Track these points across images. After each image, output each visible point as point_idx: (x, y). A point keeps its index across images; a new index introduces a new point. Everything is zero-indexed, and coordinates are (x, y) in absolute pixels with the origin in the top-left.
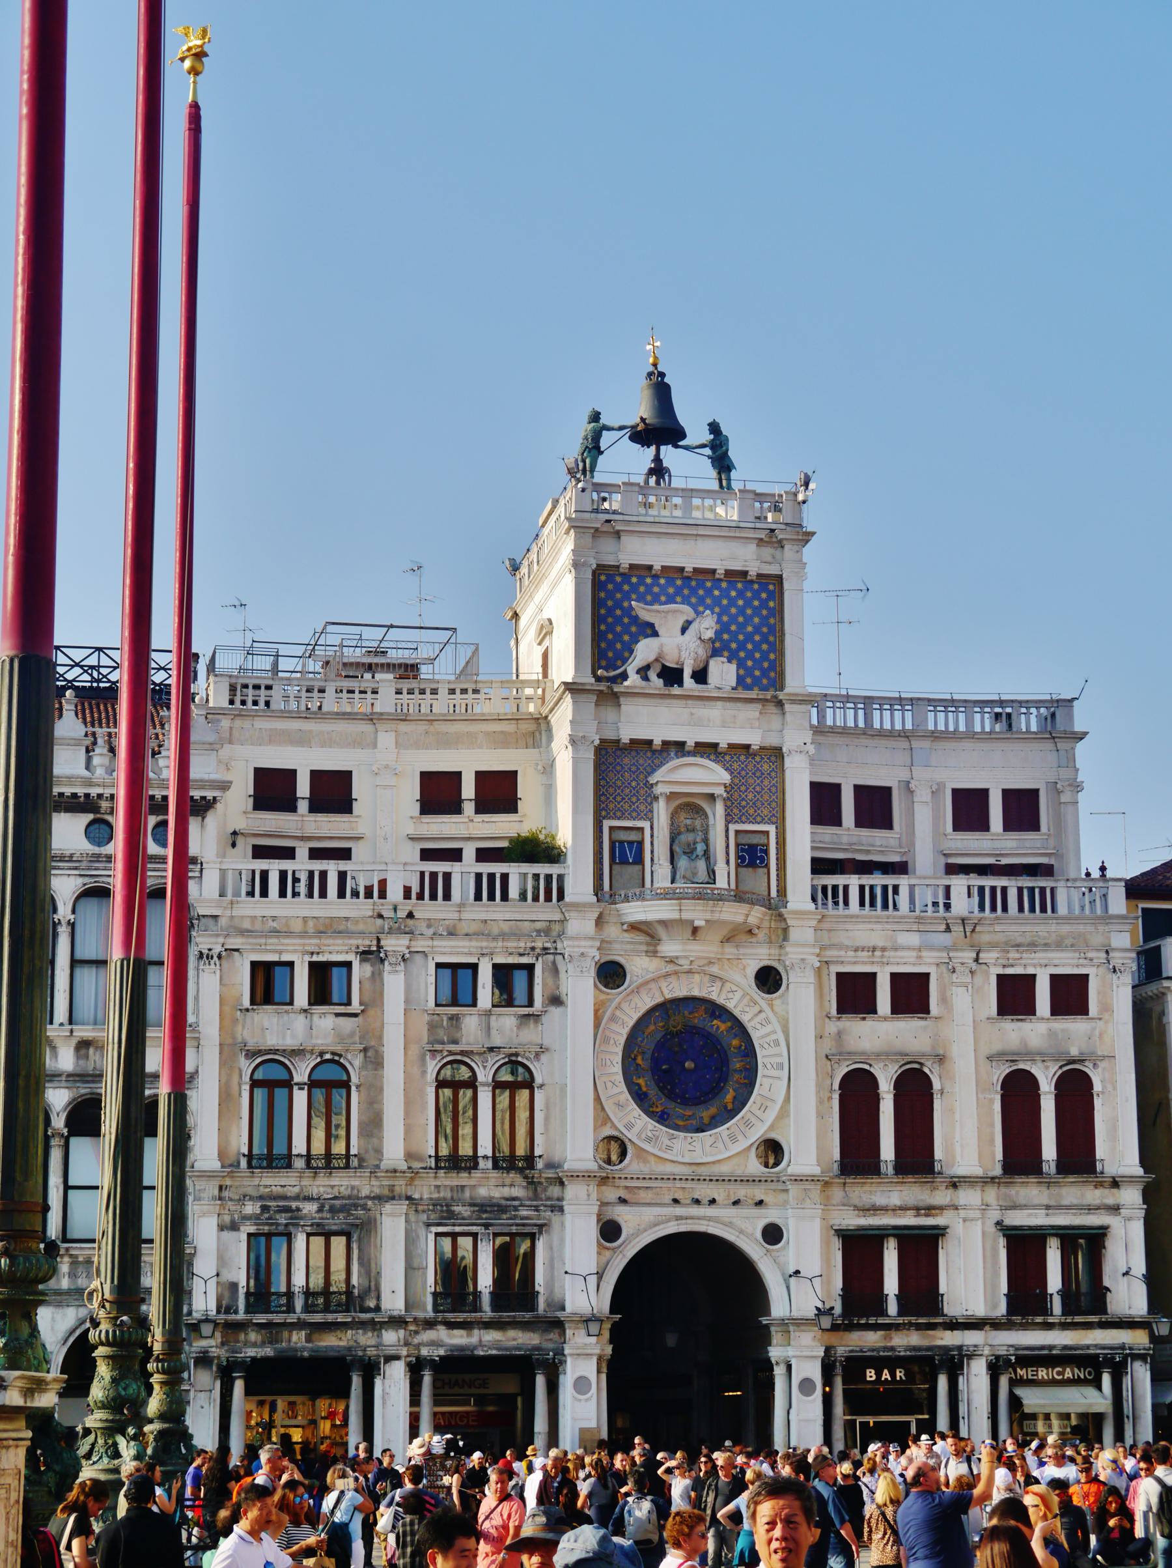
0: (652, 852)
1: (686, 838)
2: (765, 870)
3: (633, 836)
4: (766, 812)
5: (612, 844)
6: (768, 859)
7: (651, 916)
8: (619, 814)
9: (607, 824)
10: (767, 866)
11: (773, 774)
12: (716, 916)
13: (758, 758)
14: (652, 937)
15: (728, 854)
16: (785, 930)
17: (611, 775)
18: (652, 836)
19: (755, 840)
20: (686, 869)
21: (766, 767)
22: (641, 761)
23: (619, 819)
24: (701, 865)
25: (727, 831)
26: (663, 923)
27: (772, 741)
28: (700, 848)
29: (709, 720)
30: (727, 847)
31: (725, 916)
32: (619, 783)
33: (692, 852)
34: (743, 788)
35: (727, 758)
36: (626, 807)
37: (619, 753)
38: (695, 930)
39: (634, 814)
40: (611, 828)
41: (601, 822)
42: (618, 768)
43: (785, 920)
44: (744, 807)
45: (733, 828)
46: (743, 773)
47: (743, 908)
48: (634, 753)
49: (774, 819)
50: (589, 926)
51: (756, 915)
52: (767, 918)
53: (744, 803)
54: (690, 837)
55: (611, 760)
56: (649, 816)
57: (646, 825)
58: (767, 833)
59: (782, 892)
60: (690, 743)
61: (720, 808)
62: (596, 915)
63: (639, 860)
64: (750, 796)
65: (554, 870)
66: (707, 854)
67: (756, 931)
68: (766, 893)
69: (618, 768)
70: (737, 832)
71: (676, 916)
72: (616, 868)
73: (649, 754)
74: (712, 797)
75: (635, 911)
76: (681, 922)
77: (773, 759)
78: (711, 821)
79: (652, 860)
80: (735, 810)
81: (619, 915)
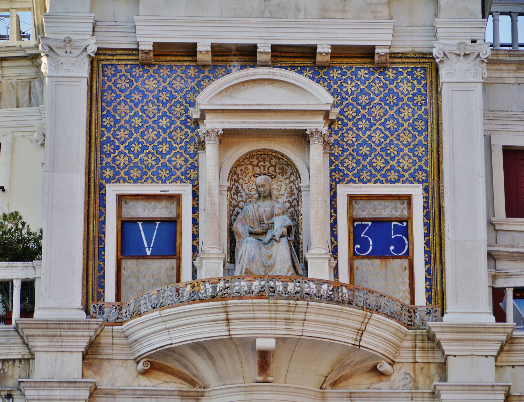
0: (195, 236)
1: (254, 209)
2: (405, 263)
3: (161, 211)
4: (405, 163)
6: (411, 243)
7: (179, 337)
8: (135, 173)
9: (112, 191)
10: (409, 256)
11: (419, 99)
12: (296, 330)
13: (390, 74)
14: (193, 383)
15: (334, 235)
16: (443, 367)
17: (123, 108)
18: (195, 210)
19: (385, 211)
20: (252, 260)
21: (405, 87)
22: (178, 84)
23: (136, 181)
24: (282, 251)
25: (333, 197)
26: (198, 347)
27: (412, 42)
28: (280, 223)
29: (298, 9)
30: (334, 225)
31: (312, 330)
33: (264, 233)
34: (364, 124)
35: (335, 74)
36: (150, 161)
37: (137, 71)
38: (264, 359)
39: (163, 173)
40: (121, 198)
41: (102, 187)
42: (137, 96)
43: (439, 345)
44: (366, 156)
45: (343, 191)
46: (364, 99)
47: (352, 316)
48: (164, 72)
49: (421, 176)
50: (72, 365)
51: (380, 334)
52: (407, 344)
53: (365, 150)
54: (264, 207)
55: (123, 83)
56: (191, 175)
57: (185, 190)
58: (408, 198)
59: (437, 299)
60: (264, 49)
61: (317, 153)
62: (84, 343)
64: (377, 137)
66: (294, 236)
67: (385, 367)
68: (407, 302)
69: (137, 96)
70: (352, 198)
71: (219, 331)
72: (129, 264)
73: (192, 72)
74: (302, 138)
75: (154, 332)
76: (230, 343)
77: (419, 73)
78: (304, 181)
79: (195, 250)
80: (348, 163)
81: (131, 345)
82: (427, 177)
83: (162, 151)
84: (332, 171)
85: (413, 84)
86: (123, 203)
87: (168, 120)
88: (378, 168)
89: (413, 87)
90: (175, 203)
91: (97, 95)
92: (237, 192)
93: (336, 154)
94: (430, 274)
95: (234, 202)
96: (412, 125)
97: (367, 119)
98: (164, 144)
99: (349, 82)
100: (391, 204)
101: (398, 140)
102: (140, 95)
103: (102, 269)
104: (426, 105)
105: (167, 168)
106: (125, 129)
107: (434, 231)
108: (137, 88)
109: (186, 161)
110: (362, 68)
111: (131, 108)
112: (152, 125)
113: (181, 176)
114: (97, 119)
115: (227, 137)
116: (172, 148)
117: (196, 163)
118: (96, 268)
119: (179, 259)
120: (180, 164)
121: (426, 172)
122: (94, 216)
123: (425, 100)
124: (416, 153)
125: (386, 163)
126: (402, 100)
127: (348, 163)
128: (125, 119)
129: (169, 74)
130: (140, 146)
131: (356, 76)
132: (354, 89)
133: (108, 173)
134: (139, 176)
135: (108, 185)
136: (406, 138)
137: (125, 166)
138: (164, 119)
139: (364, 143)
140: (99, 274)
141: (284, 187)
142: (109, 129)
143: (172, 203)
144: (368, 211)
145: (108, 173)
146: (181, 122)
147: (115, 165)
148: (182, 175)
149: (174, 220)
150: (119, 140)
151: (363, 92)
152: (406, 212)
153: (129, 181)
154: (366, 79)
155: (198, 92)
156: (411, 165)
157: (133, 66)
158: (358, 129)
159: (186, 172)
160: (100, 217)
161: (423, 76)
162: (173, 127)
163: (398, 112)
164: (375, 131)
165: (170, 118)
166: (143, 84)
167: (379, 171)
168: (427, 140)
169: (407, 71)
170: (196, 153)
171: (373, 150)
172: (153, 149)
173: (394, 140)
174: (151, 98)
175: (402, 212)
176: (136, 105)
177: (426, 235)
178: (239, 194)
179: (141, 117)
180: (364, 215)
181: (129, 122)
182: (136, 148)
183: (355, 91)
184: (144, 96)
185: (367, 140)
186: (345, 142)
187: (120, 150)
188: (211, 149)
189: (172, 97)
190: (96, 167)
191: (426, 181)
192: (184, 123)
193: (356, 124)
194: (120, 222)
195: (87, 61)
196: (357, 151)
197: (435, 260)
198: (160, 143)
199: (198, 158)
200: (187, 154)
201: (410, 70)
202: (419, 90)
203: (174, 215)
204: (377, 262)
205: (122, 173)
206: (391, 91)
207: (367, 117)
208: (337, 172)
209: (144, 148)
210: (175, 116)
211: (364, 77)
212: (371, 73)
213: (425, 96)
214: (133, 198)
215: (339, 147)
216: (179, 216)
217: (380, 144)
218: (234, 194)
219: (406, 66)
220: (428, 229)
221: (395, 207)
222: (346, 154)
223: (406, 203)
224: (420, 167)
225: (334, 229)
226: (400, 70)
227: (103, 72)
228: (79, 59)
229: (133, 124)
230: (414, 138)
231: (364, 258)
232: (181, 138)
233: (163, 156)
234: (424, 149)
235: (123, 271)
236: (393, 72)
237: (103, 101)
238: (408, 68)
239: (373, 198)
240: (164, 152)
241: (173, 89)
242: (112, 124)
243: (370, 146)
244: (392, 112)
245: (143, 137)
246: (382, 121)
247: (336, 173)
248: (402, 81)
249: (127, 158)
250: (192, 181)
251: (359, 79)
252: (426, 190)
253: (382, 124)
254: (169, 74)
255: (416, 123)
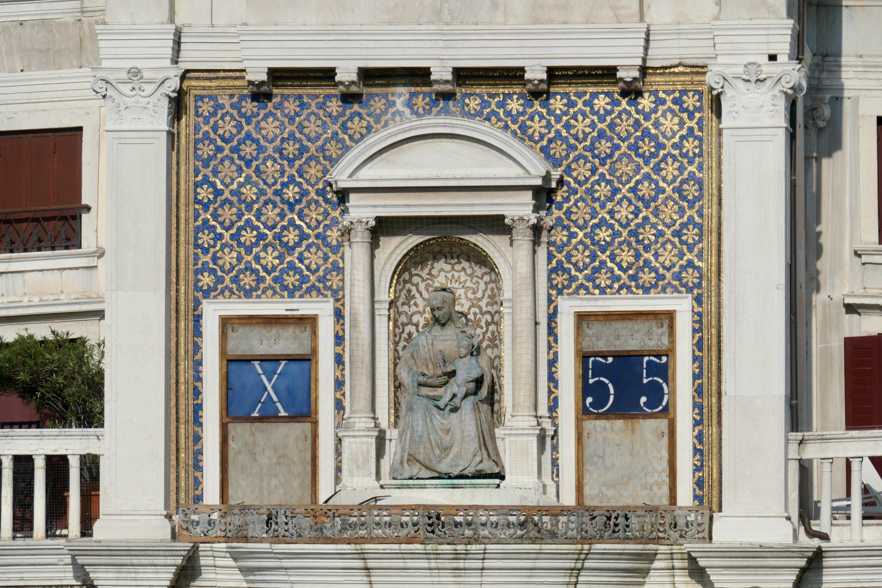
0: (339, 384)
2: (663, 424)
4: (667, 257)
5: (232, 363)
6: (673, 393)
8: (248, 280)
9: (213, 311)
10: (668, 412)
11: (689, 146)
13: (646, 102)
17: (227, 169)
19: (631, 339)
21: (669, 123)
22: (312, 128)
23: (248, 294)
24: (466, 422)
25: (552, 317)
28: (466, 370)
32: (250, 193)
34: (603, 190)
36: (270, 258)
37: (249, 106)
39: (291, 280)
40: (226, 322)
41: (197, 303)
42: (248, 150)
45: (569, 307)
46: (604, 147)
49: (690, 277)
53: (603, 235)
55: (228, 127)
57: (321, 309)
58: (670, 316)
63: (303, 412)
64: (624, 212)
65: (70, 442)
69: (248, 150)
70: (582, 318)
72: (238, 430)
80: (578, 257)
82: (701, 278)
83: (288, 242)
84: (551, 271)
85: (681, 119)
86: (230, 330)
87: (297, 189)
88: (625, 265)
89: (681, 124)
90: (309, 330)
91: (188, 149)
92: (410, 297)
93: (559, 243)
94: (701, 442)
95: (403, 319)
96: (679, 190)
97: (609, 182)
98: (291, 229)
99: (580, 118)
100: (641, 326)
101: (657, 216)
102: (254, 146)
103: (198, 439)
104: (700, 155)
105: (298, 271)
106: (232, 204)
107: (710, 370)
108: (248, 136)
109: (326, 258)
110: (603, 93)
111: (240, 170)
112: (273, 198)
113: (317, 284)
114: (187, 190)
115: (383, 227)
116: (303, 237)
117: (340, 261)
118: (191, 439)
119: (315, 423)
120: (316, 264)
121: (699, 269)
122: (186, 352)
123: (700, 146)
124: (684, 238)
125: (637, 256)
126: (663, 147)
127: (578, 257)
128: (232, 187)
129: (298, 109)
130: (255, 233)
131: (592, 108)
132: (588, 130)
133: (207, 280)
134: (254, 284)
135: (204, 301)
136: (669, 212)
137: (233, 268)
138: (291, 187)
139: (603, 223)
140: (196, 448)
141: (482, 286)
142: (206, 207)
143: (303, 329)
144: (607, 340)
145: (207, 280)
146: (318, 193)
147: (215, 267)
148: (319, 281)
149: (307, 358)
150: (222, 224)
151: (601, 135)
152: (665, 341)
153: (237, 292)
154: (608, 113)
155: (333, 161)
156: (675, 259)
157: (242, 98)
158: (595, 200)
159: (324, 276)
160: (195, 354)
161: (698, 104)
162: (304, 201)
163: (657, 169)
164: (620, 203)
165: (299, 185)
166: (259, 129)
167: (625, 271)
168: (701, 216)
169: (672, 97)
170: (340, 245)
171: (616, 234)
172: (274, 238)
173: (651, 216)
174: (270, 151)
175: (660, 339)
176: (248, 164)
177: (696, 377)
178: (412, 303)
179: (256, 185)
180: (601, 346)
181: (236, 193)
182: (248, 236)
183: (590, 133)
184: (260, 149)
185: (608, 217)
186: (573, 221)
187: (224, 241)
188: (356, 255)
189: (303, 149)
190: (187, 270)
191: (699, 285)
192: (321, 193)
193: (590, 192)
194: (225, 363)
195: (165, 103)
196: (590, 236)
197: (710, 418)
198: (284, 228)
199: (343, 254)
200: (326, 246)
201: (677, 95)
202: (691, 129)
203: (305, 350)
204: (619, 423)
205: (227, 279)
206: (646, 133)
207: (608, 177)
208: (560, 273)
209: (261, 237)
210: (308, 182)
211: (605, 109)
212: (615, 103)
213: (700, 139)
214: (244, 321)
215: (562, 230)
216: (314, 351)
217: (628, 224)
218: (403, 304)
219: (671, 88)
220: (701, 367)
221: (649, 332)
222: (574, 241)
223: (666, 326)
224: (690, 263)
225: (554, 369)
226: (662, 95)
227: (197, 107)
228: (153, 99)
229: (243, 197)
230: (681, 211)
231: (599, 416)
232: (317, 220)
233: (291, 250)
234: (696, 230)
235: (230, 442)
236: (650, 99)
237: (197, 157)
238: (674, 92)
239: (614, 317)
240: (291, 244)
241: (305, 135)
242: (211, 197)
243: (611, 227)
244: (646, 170)
245: (258, 219)
246: (632, 184)
247: (558, 275)
248: (664, 115)
249: (234, 254)
250: (335, 293)
251: (597, 113)
252: (698, 300)
253: (633, 190)
254: (298, 109)
255: (685, 187)
